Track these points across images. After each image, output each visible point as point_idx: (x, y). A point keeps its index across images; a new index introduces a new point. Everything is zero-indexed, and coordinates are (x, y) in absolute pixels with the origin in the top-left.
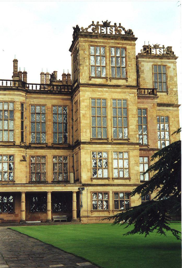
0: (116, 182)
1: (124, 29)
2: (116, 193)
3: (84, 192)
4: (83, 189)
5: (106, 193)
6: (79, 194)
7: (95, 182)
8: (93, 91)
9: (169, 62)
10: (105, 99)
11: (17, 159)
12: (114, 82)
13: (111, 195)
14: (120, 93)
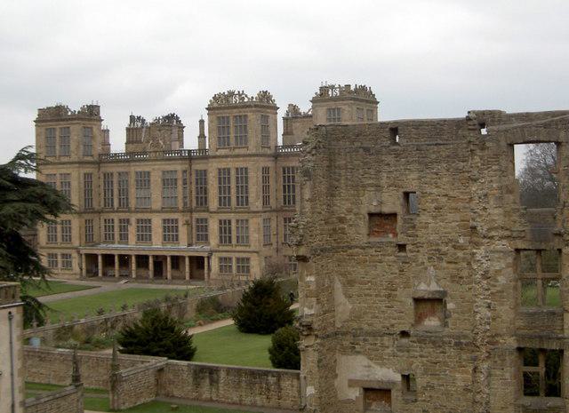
0: (238, 248)
1: (246, 96)
2: (238, 259)
3: (213, 257)
4: (212, 254)
5: (230, 259)
6: (209, 258)
7: (221, 248)
8: (219, 162)
9: (345, 104)
10: (229, 170)
11: (180, 224)
12: (237, 151)
13: (234, 260)
14: (241, 161)
